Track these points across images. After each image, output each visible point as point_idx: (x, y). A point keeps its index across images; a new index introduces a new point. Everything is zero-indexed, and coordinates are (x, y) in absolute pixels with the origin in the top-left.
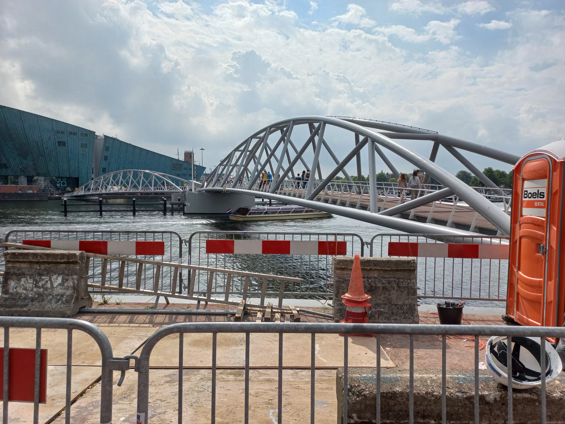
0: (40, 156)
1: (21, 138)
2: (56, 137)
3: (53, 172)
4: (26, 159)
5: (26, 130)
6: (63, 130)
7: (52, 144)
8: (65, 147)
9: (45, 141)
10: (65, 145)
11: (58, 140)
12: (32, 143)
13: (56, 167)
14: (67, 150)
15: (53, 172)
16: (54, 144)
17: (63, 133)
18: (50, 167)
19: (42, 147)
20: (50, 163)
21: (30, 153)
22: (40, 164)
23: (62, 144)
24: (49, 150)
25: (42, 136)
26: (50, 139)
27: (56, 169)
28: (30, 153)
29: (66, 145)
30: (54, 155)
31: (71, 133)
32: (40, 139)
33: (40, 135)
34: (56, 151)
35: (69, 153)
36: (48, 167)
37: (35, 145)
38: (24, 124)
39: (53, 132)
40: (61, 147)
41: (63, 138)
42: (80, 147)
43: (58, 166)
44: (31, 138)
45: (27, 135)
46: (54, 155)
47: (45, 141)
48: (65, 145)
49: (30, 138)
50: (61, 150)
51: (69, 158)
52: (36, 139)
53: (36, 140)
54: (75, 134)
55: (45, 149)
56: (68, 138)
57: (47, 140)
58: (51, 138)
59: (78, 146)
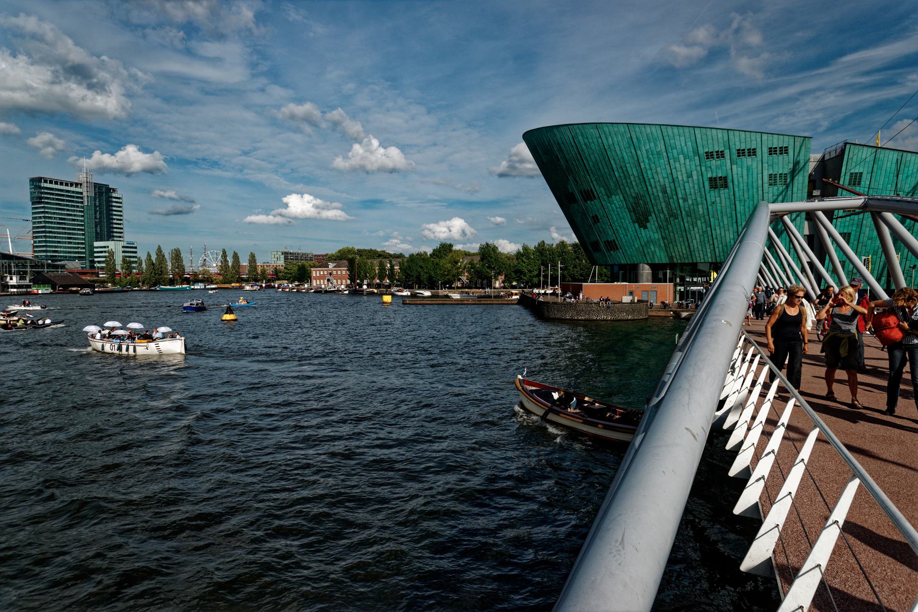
0: (672, 219)
1: (634, 183)
2: (703, 168)
3: (701, 252)
4: (645, 227)
5: (642, 165)
6: (721, 150)
7: (696, 187)
8: (726, 190)
9: (681, 182)
10: (726, 186)
11: (710, 175)
12: (655, 190)
13: (706, 239)
14: (732, 197)
15: (701, 252)
16: (702, 186)
17: (721, 155)
18: (694, 241)
19: (675, 197)
20: (692, 232)
21: (653, 214)
22: (672, 234)
23: (719, 183)
24: (690, 202)
25: (674, 171)
26: (690, 176)
27: (707, 245)
28: (653, 214)
29: (730, 185)
30: (701, 213)
31: (740, 153)
32: (671, 180)
33: (669, 172)
34: (705, 201)
35: (737, 203)
36: (690, 241)
37: (660, 195)
38: (639, 152)
39: (697, 158)
40: (717, 190)
41: (717, 168)
42: (766, 186)
43: (710, 238)
44: (652, 180)
45: (645, 176)
46: (701, 213)
47: (681, 182)
48: (726, 186)
49: (650, 182)
50: (718, 199)
51: (738, 215)
52: (661, 180)
53: (662, 183)
54: (752, 152)
55: (681, 201)
56: (734, 167)
57: (685, 179)
58: (694, 173)
59: (760, 182)
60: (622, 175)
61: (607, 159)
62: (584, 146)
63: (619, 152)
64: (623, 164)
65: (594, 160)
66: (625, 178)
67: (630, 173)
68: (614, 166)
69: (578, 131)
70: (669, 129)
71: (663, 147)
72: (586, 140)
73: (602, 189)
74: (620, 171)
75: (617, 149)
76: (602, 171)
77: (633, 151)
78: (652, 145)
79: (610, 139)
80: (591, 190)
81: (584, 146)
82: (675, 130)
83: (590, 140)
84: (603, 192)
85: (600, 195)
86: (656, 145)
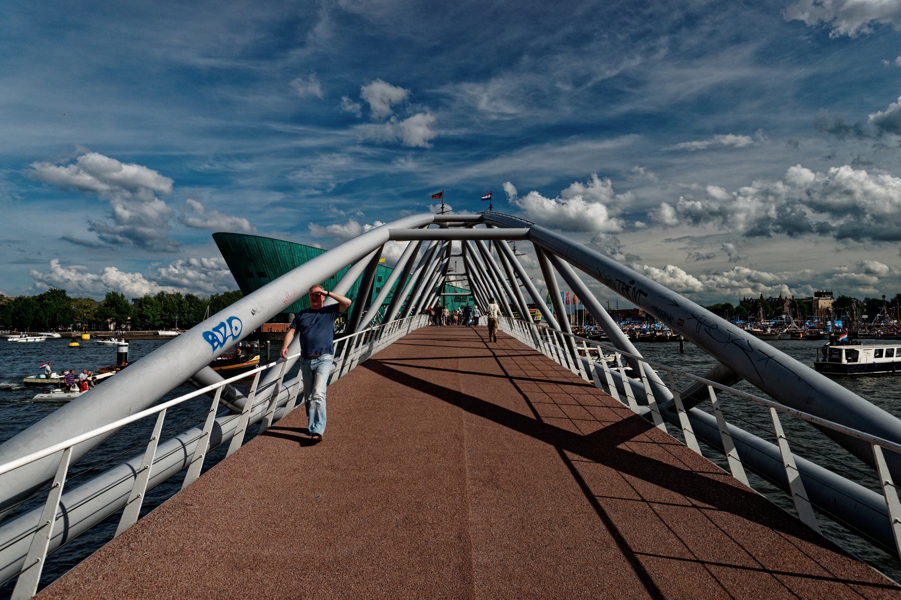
38: (294, 257)
60: (284, 267)
61: (276, 257)
62: (263, 249)
63: (283, 255)
64: (285, 261)
65: (268, 256)
66: (286, 269)
67: (289, 266)
68: (280, 261)
69: (261, 241)
70: (310, 248)
71: (306, 256)
72: (265, 246)
73: (271, 272)
74: (284, 265)
75: (283, 253)
76: (273, 263)
77: (291, 256)
78: (301, 254)
79: (279, 248)
80: (265, 272)
81: (263, 249)
82: (313, 249)
83: (268, 247)
84: (272, 274)
85: (270, 275)
86: (303, 254)
